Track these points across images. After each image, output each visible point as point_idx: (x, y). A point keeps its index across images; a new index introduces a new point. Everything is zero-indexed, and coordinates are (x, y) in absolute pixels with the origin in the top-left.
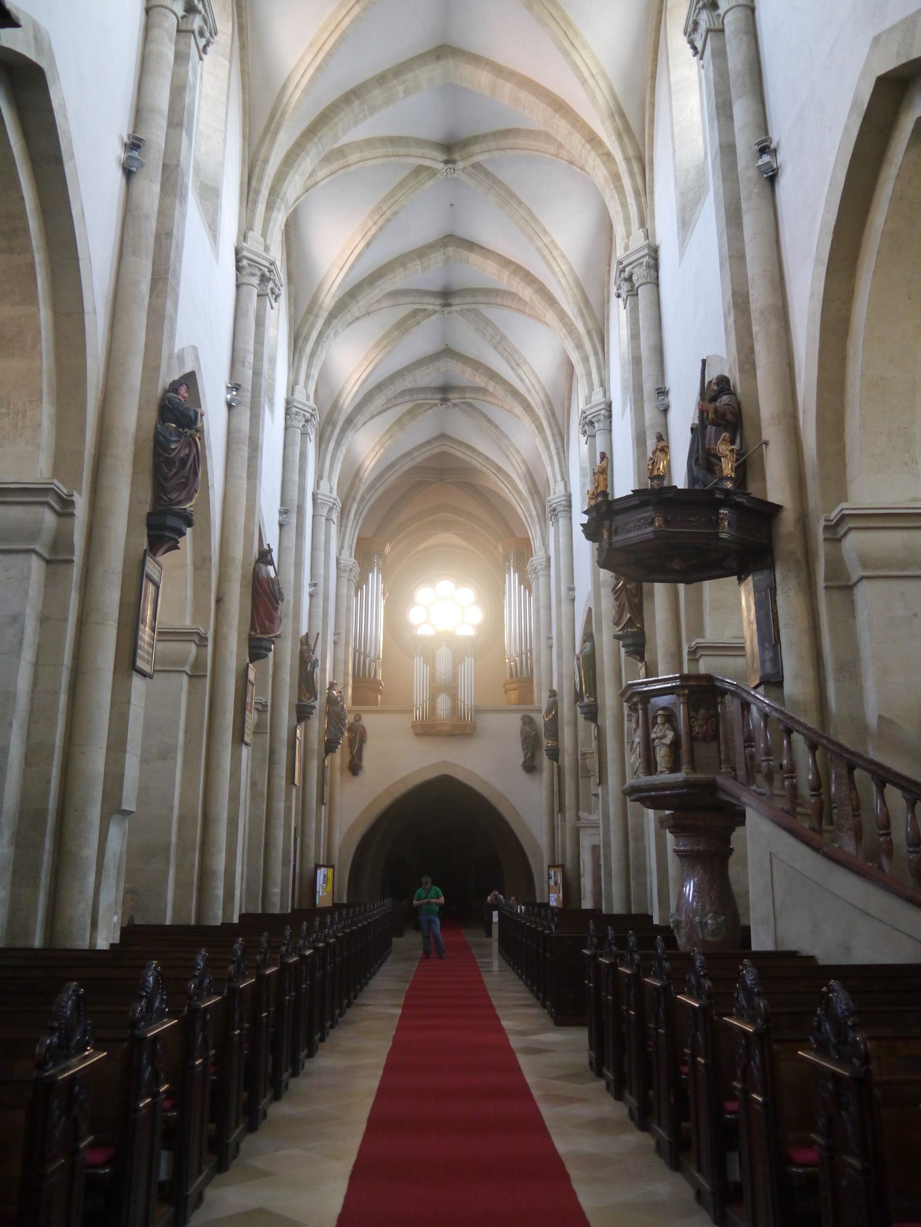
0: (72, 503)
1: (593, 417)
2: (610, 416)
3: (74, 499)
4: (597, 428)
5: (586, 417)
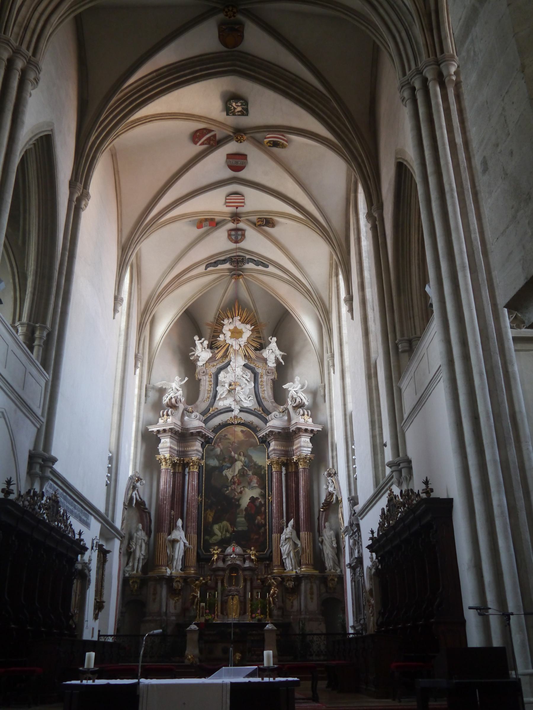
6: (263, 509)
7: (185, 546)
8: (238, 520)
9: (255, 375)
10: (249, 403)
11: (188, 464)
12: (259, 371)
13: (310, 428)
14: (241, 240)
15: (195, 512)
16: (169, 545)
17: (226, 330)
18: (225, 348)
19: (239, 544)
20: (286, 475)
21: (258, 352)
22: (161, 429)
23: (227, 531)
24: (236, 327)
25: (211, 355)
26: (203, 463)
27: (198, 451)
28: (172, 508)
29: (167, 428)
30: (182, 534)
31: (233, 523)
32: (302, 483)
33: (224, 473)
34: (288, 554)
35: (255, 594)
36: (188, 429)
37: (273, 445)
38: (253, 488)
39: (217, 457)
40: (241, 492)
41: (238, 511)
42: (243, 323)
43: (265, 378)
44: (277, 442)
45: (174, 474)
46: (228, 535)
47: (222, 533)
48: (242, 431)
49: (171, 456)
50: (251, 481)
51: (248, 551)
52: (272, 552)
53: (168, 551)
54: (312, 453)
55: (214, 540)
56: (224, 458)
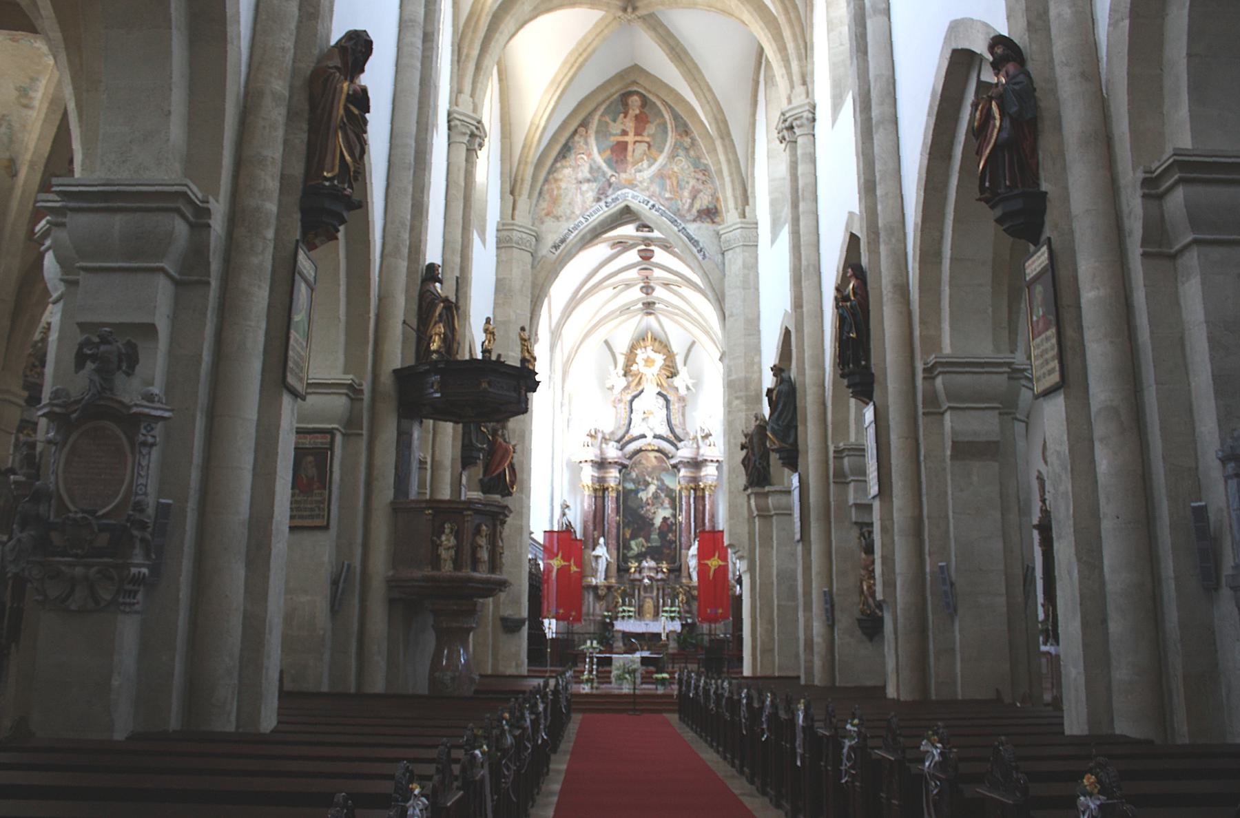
0: (207, 212)
1: (796, 119)
2: (814, 120)
3: (210, 206)
4: (798, 133)
5: (785, 121)
6: (674, 527)
7: (607, 559)
8: (652, 537)
9: (667, 401)
10: (664, 430)
11: (607, 489)
12: (671, 397)
13: (715, 459)
14: (651, 293)
15: (614, 531)
16: (592, 558)
17: (638, 360)
18: (639, 377)
19: (652, 558)
20: (695, 498)
21: (670, 379)
22: (583, 460)
23: (643, 546)
24: (648, 357)
25: (625, 384)
26: (621, 488)
27: (616, 477)
28: (595, 529)
29: (589, 459)
30: (605, 549)
31: (648, 539)
32: (707, 507)
33: (639, 495)
34: (694, 569)
35: (666, 599)
36: (606, 459)
37: (683, 472)
38: (665, 508)
39: (633, 481)
40: (654, 513)
41: (652, 529)
42: (655, 352)
43: (677, 406)
44: (687, 470)
45: (596, 497)
46: (644, 549)
47: (638, 547)
48: (656, 457)
49: (593, 483)
50: (663, 502)
51: (660, 565)
52: (681, 566)
53: (594, 565)
54: (717, 480)
55: (631, 554)
56: (639, 482)
